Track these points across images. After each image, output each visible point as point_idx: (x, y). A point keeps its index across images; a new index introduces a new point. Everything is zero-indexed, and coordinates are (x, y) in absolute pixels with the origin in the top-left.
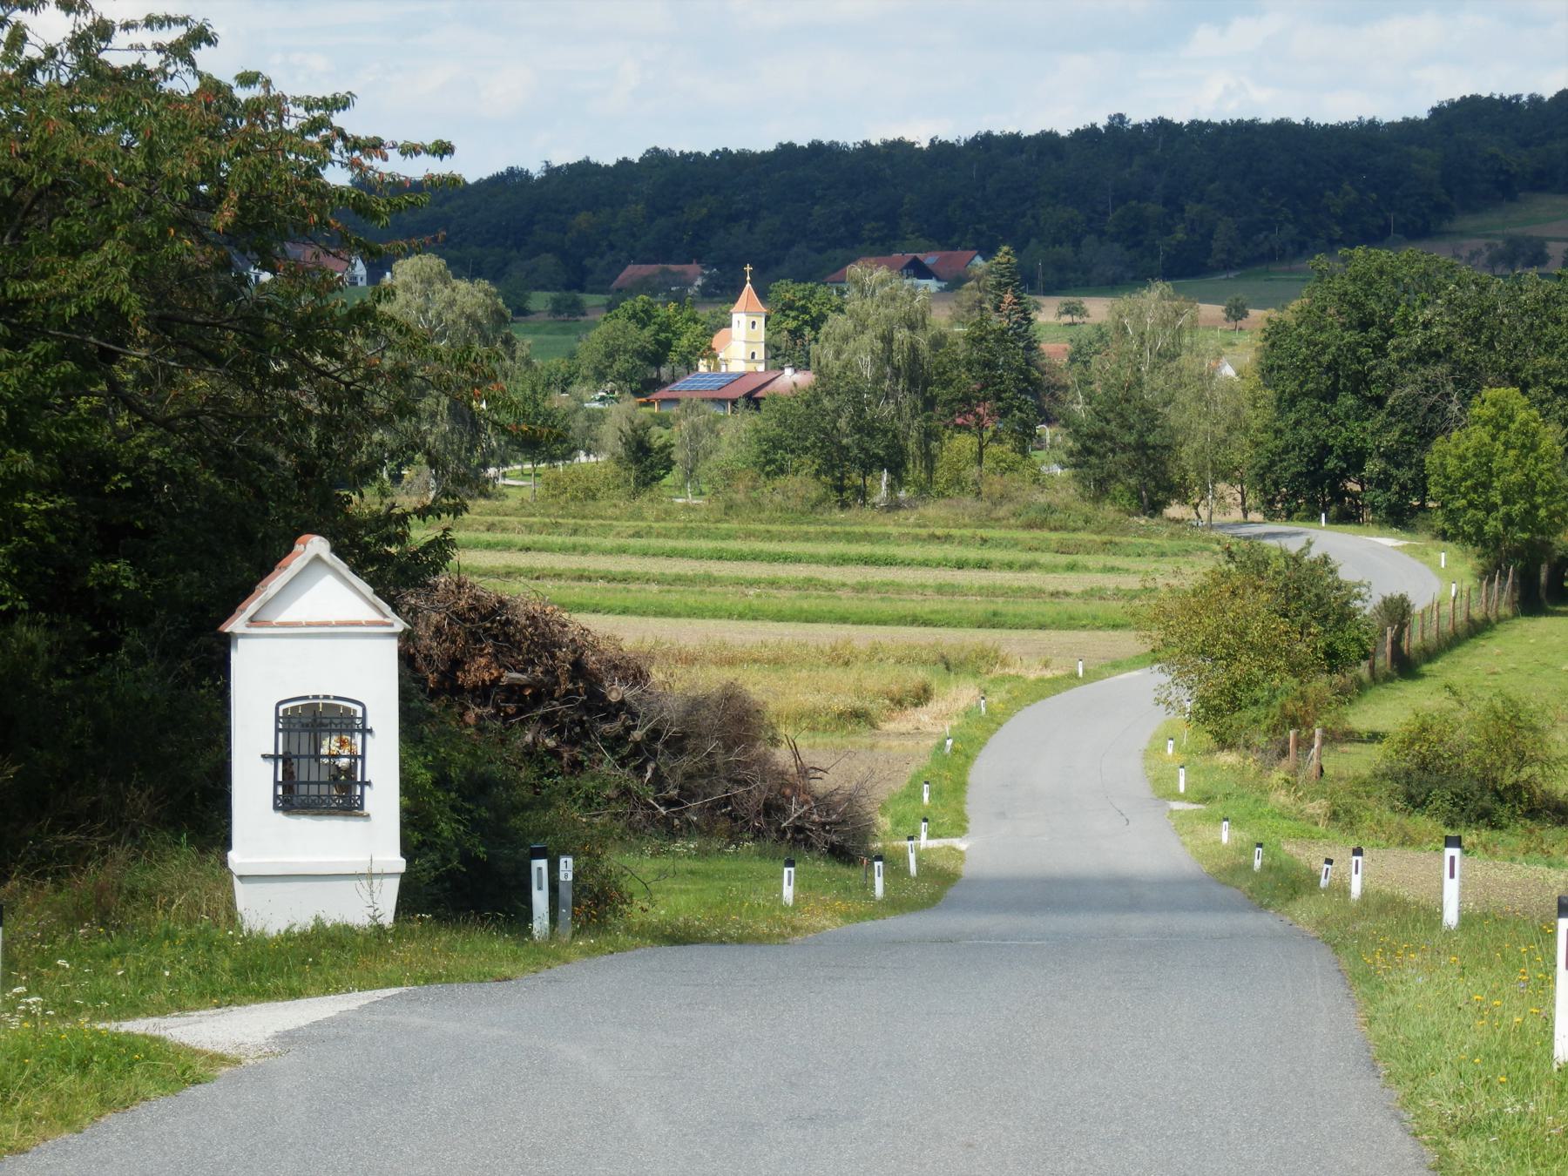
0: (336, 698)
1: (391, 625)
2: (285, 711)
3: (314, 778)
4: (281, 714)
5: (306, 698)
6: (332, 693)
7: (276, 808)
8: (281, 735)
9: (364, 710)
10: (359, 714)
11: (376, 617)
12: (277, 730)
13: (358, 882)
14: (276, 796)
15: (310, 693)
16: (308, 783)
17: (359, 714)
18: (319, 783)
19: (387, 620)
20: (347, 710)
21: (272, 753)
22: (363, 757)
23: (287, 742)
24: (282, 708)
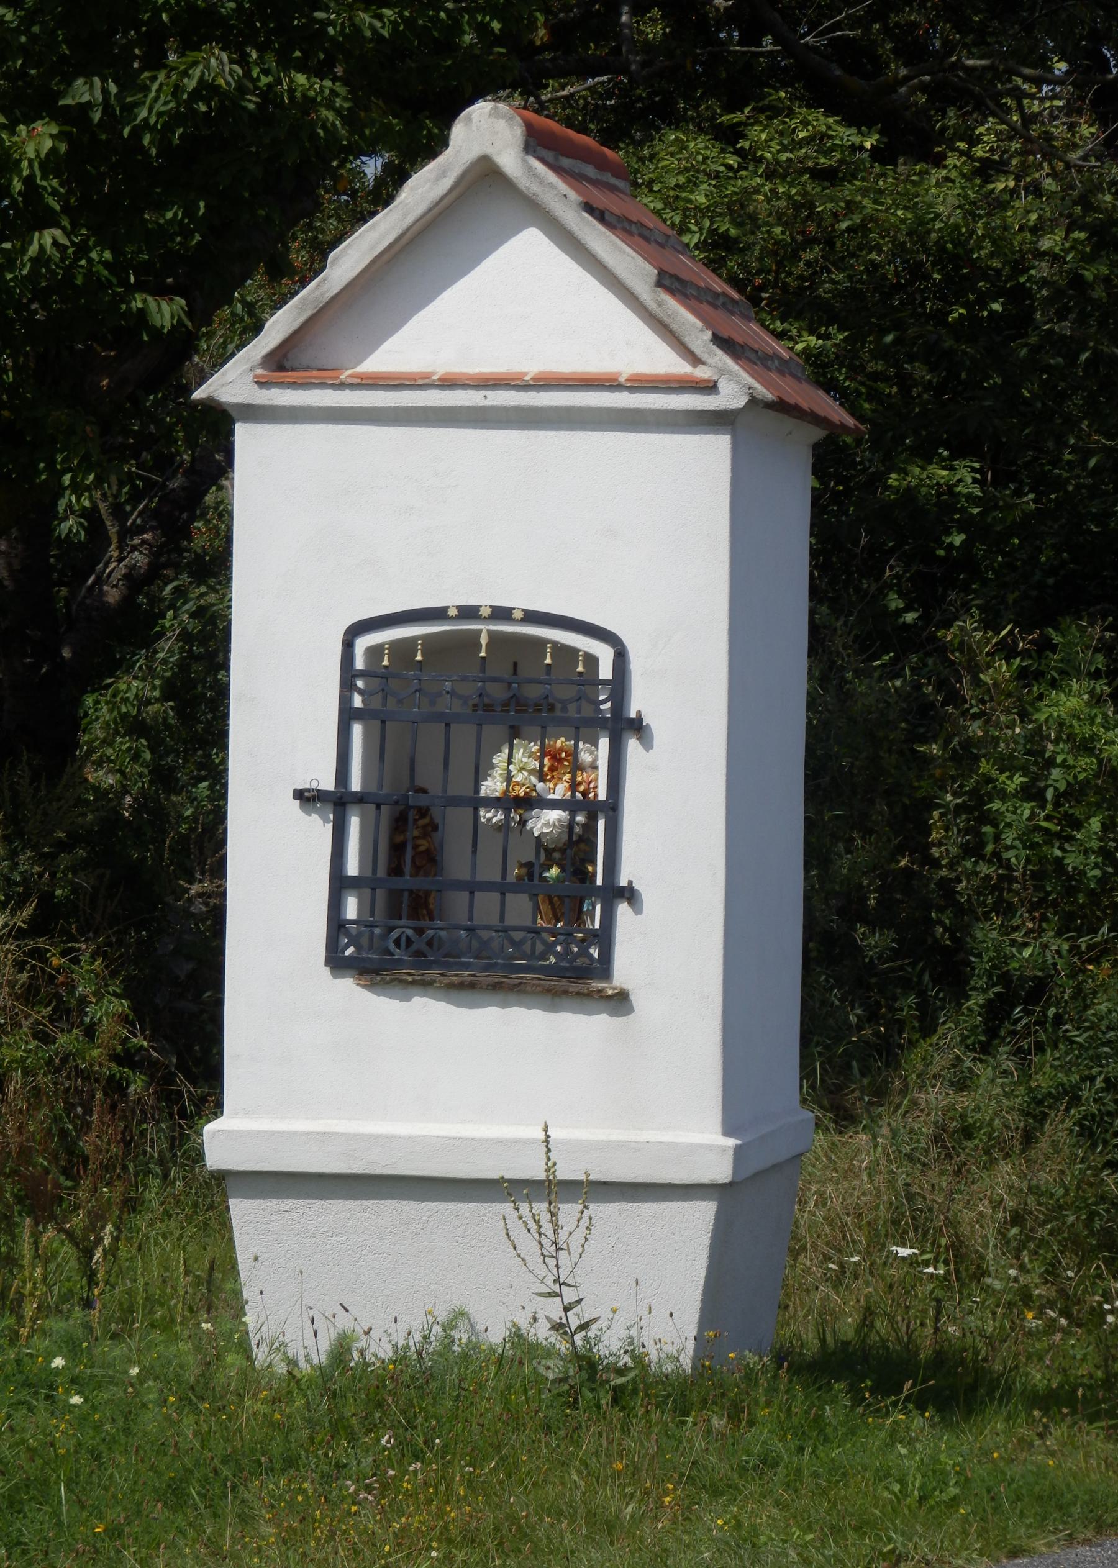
0: (532, 617)
1: (710, 388)
2: (374, 652)
3: (489, 872)
4: (359, 664)
5: (437, 614)
6: (519, 602)
7: (336, 962)
8: (357, 730)
9: (621, 657)
10: (606, 671)
11: (680, 367)
12: (347, 716)
13: (507, 1208)
14: (336, 924)
15: (452, 599)
16: (472, 887)
17: (606, 671)
18: (502, 888)
19: (702, 373)
20: (566, 653)
21: (328, 783)
22: (613, 808)
23: (377, 752)
24: (362, 644)
